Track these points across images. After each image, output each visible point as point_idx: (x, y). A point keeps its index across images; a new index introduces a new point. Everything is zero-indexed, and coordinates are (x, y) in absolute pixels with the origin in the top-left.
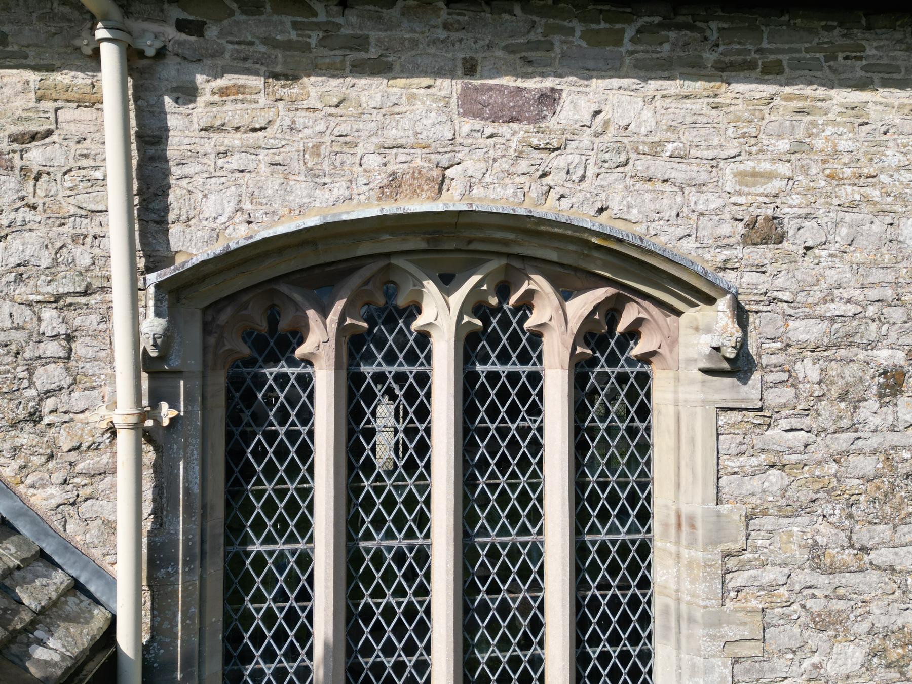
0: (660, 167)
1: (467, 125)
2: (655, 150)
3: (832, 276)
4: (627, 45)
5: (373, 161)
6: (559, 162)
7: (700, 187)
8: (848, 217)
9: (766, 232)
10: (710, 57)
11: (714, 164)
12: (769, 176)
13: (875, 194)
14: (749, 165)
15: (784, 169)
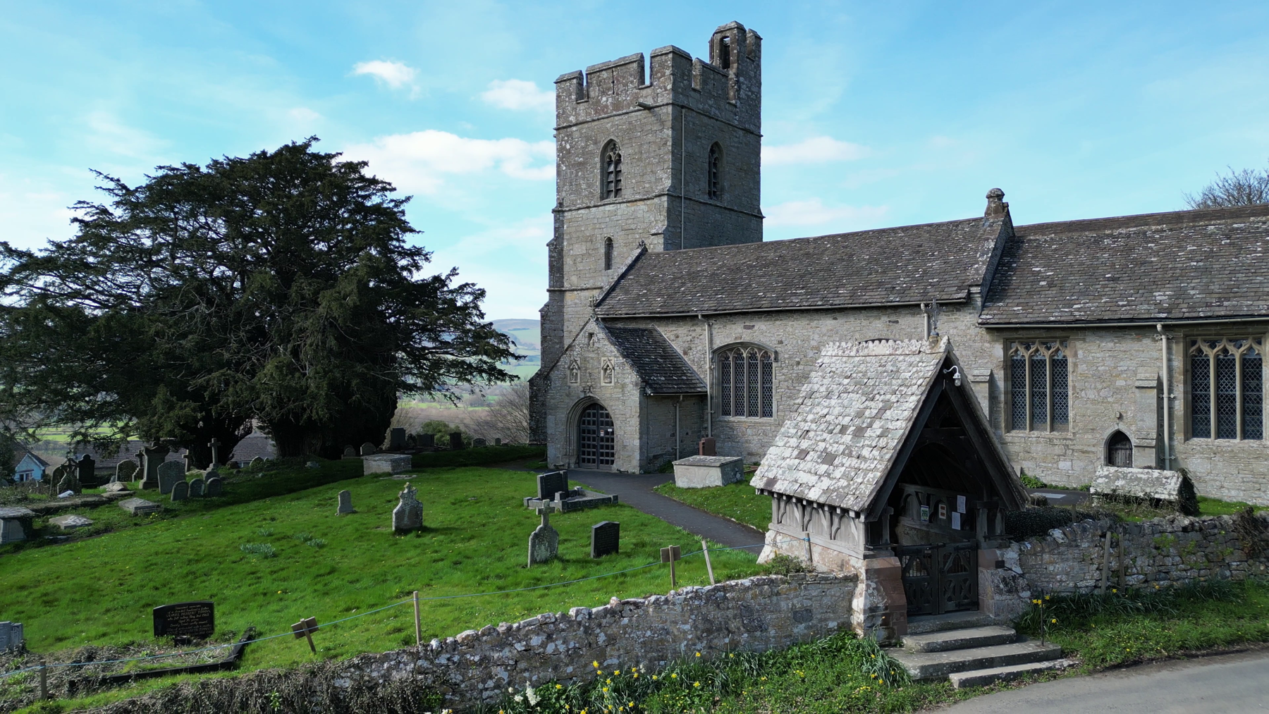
9: (781, 342)
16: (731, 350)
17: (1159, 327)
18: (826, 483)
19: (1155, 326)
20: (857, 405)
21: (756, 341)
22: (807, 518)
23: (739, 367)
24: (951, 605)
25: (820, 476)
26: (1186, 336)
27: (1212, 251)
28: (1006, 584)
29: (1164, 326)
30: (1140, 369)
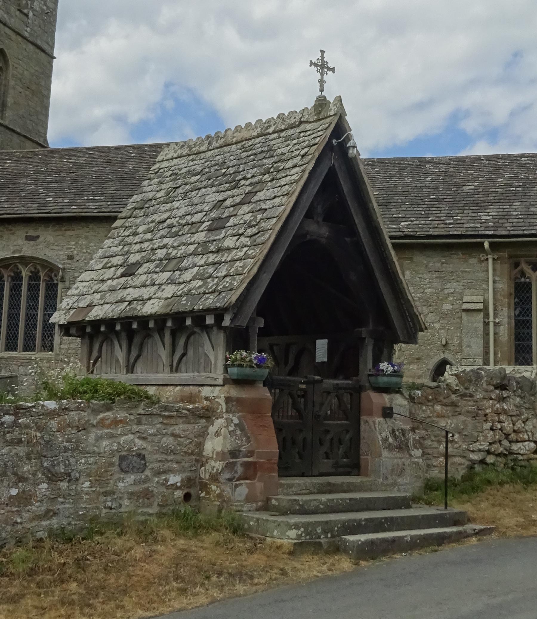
0: (54, 247)
1: (26, 242)
2: (53, 244)
3: (81, 265)
4: (50, 228)
5: (12, 248)
6: (39, 247)
7: (60, 250)
8: (84, 255)
9: (71, 257)
10: (63, 229)
11: (63, 247)
12: (71, 248)
13: (89, 251)
14: (68, 246)
15: (74, 247)
16: (6, 267)
17: (486, 245)
18: (169, 291)
19: (482, 244)
20: (213, 197)
21: (40, 255)
22: (134, 354)
23: (16, 289)
24: (326, 464)
25: (160, 285)
26: (510, 257)
27: (528, 178)
28: (395, 437)
29: (491, 244)
30: (467, 292)
